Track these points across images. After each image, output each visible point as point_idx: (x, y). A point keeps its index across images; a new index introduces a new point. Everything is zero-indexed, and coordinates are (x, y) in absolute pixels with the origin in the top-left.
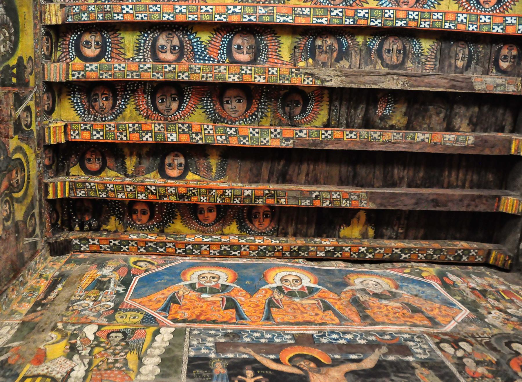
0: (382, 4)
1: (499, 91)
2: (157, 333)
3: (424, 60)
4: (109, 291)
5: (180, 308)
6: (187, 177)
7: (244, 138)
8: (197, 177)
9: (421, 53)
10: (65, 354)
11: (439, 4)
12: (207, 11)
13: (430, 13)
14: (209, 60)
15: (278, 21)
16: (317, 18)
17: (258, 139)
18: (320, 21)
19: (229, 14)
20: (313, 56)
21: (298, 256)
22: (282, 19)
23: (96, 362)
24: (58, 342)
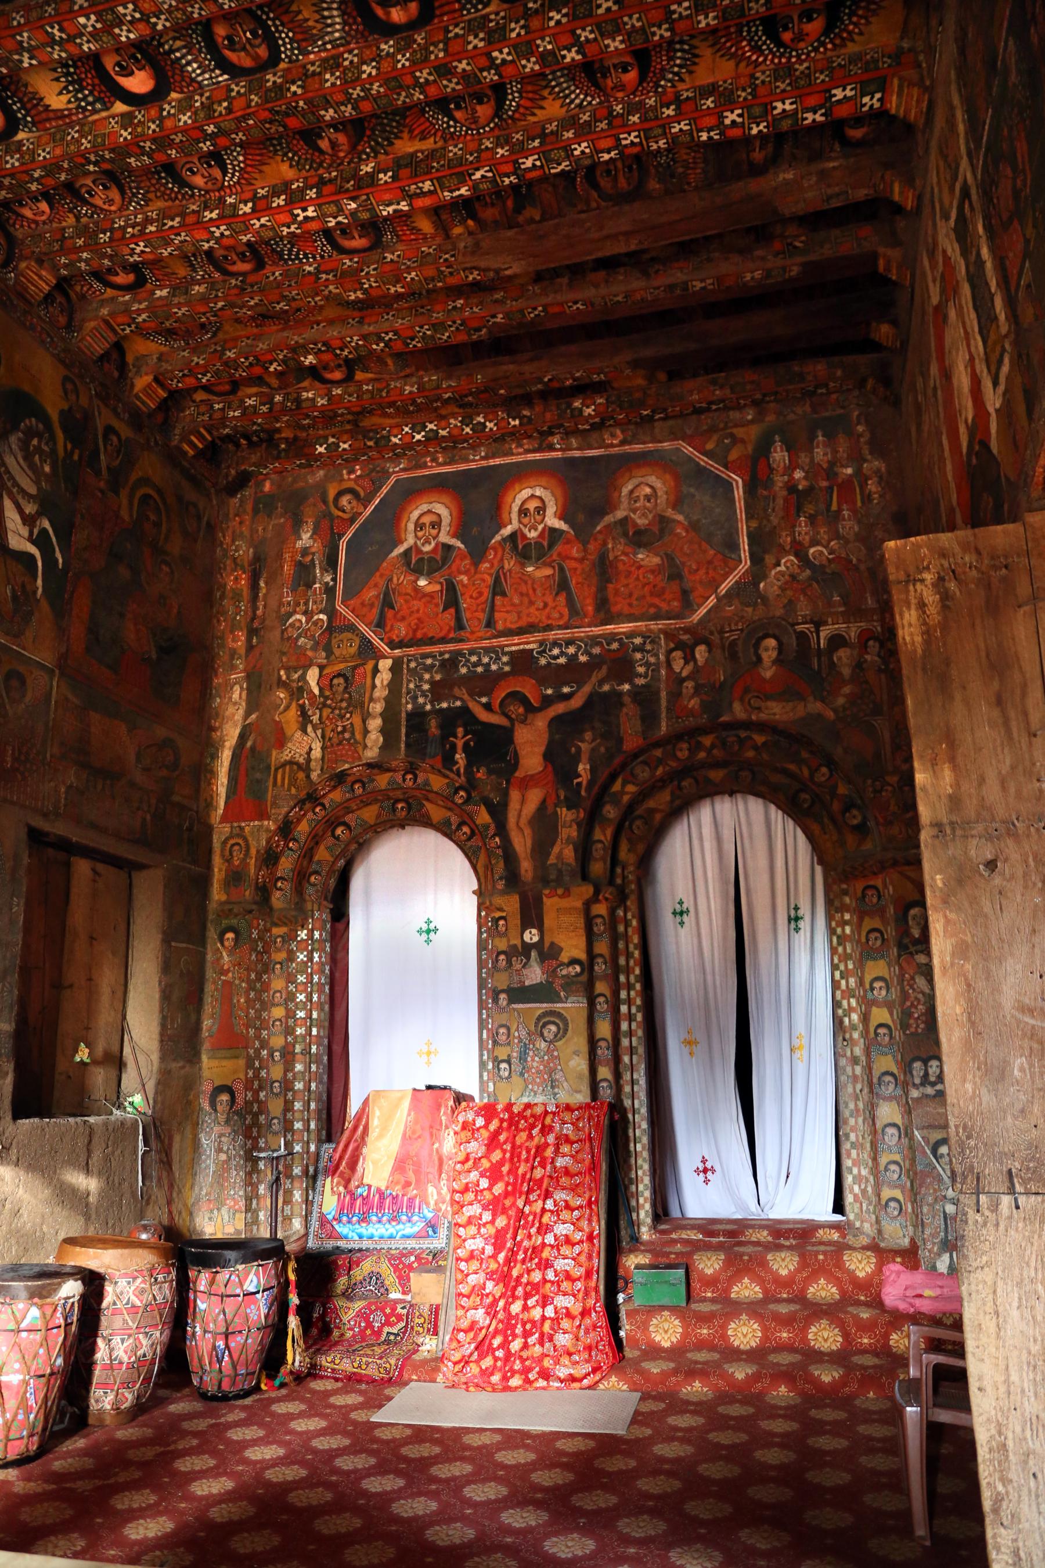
0: (572, 101)
1: (835, 203)
2: (376, 671)
3: (681, 170)
4: (317, 585)
7: (413, 339)
8: (370, 375)
9: (673, 159)
11: (690, 72)
12: (262, 226)
13: (663, 126)
15: (385, 213)
16: (451, 191)
17: (432, 337)
18: (457, 193)
19: (301, 223)
20: (473, 216)
21: (552, 434)
22: (391, 209)
23: (329, 734)
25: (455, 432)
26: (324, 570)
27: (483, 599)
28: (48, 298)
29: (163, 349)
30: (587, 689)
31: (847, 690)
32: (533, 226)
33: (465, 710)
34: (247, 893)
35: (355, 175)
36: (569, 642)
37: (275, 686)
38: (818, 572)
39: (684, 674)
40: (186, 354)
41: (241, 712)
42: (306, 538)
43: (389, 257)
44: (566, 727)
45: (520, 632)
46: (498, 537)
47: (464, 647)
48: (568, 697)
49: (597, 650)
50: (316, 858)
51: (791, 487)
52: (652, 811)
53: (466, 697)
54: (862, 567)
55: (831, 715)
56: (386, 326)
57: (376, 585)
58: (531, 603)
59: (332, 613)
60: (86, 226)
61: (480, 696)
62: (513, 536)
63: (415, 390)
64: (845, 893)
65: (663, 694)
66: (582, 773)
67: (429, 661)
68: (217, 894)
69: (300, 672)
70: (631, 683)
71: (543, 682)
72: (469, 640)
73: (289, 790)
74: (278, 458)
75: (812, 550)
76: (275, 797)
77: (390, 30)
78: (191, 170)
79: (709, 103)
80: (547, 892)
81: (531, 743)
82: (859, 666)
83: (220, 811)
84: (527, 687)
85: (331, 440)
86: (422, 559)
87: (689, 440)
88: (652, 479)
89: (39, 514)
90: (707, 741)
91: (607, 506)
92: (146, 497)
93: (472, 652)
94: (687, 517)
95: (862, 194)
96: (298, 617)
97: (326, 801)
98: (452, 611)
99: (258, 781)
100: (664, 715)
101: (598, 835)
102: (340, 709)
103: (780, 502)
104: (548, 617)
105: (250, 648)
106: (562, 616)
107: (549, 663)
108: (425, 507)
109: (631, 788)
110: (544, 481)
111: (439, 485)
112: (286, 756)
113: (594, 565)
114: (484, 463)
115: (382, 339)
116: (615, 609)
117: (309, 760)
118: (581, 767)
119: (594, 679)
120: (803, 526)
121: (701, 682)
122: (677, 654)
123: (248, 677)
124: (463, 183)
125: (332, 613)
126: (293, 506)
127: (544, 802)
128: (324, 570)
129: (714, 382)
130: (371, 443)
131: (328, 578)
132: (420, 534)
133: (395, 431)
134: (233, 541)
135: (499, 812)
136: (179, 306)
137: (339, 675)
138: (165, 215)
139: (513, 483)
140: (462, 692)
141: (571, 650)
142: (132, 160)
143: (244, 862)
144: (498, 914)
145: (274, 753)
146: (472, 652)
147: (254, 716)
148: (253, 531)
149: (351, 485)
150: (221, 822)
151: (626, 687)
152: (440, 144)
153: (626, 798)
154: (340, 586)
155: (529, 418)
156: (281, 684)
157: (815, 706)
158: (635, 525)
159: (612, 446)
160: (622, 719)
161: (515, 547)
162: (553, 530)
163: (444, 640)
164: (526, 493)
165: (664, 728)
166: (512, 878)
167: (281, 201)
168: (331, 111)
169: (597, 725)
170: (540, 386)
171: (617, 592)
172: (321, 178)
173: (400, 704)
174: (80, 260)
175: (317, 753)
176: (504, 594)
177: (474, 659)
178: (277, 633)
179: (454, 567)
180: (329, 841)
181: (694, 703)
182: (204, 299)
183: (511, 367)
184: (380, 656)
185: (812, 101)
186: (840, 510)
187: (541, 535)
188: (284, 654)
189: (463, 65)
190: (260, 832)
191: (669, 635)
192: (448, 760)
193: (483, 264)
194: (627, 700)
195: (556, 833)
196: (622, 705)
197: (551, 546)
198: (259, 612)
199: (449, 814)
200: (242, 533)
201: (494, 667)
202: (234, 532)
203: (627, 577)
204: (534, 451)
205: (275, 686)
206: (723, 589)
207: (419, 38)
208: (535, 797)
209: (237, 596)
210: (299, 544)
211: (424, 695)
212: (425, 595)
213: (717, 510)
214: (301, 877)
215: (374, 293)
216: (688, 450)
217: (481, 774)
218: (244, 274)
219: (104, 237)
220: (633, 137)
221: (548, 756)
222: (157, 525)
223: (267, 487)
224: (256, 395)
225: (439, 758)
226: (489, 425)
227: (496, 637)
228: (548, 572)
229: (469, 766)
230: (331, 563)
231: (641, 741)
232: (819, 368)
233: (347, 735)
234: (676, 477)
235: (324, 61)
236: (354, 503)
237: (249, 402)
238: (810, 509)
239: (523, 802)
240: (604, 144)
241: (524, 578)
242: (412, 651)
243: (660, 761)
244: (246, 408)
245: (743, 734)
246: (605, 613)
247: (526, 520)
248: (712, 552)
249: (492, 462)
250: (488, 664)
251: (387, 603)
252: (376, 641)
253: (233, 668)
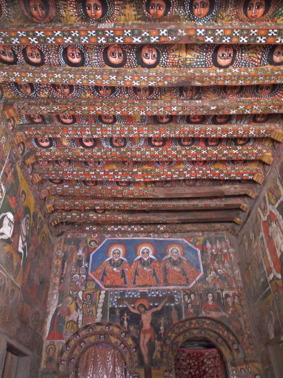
2: (100, 294)
4: (83, 267)
5: (106, 278)
6: (106, 213)
10: (75, 309)
14: (109, 185)
21: (151, 233)
24: (72, 303)
25: (126, 229)
26: (85, 262)
28: (36, 184)
29: (57, 198)
30: (162, 304)
31: (231, 309)
32: (168, 188)
33: (127, 308)
34: (54, 366)
35: (132, 171)
36: (157, 290)
37: (68, 296)
38: (221, 276)
39: (189, 302)
40: (63, 200)
41: (56, 303)
42: (80, 252)
43: (131, 189)
44: (157, 315)
45: (143, 286)
46: (136, 259)
47: (127, 289)
48: (157, 306)
49: (164, 293)
50: (74, 353)
51: (212, 254)
52: (178, 342)
53: (127, 304)
54: (231, 276)
55: (228, 317)
56: (121, 203)
57: (101, 268)
58: (146, 278)
59: (87, 275)
60: (56, 169)
61: (132, 304)
62: (140, 259)
63: (121, 218)
64: (234, 370)
65: (183, 307)
67: (116, 292)
68: (43, 366)
69: (76, 292)
70: (174, 303)
71: (150, 301)
73: (71, 330)
74: (74, 229)
75: (218, 271)
76: (66, 332)
77: (154, 146)
78: (91, 163)
79: (218, 172)
80: (152, 368)
81: (146, 319)
82: (233, 303)
83: (47, 336)
84: (145, 302)
85: (91, 226)
86: (115, 263)
87: (186, 239)
88: (177, 248)
89: (25, 241)
90: (194, 321)
91: (166, 254)
92: (43, 237)
93: (129, 291)
94: (186, 259)
95: (242, 193)
96: (77, 275)
97: (80, 334)
99: (60, 326)
100: (184, 314)
101: (165, 349)
102: (89, 305)
103: (210, 257)
104: (151, 283)
105: (60, 283)
106: (154, 283)
107: (151, 296)
108: (115, 248)
109: (173, 335)
110: (149, 245)
111: (120, 242)
112: (70, 318)
113: (163, 269)
114: (132, 238)
115: (119, 206)
116: (169, 282)
117: (78, 320)
118: (161, 328)
119: (164, 302)
120: (216, 264)
121: (194, 304)
122: (186, 296)
123: (60, 292)
124: (158, 178)
125: (87, 275)
126: (77, 243)
127: (151, 338)
128: (85, 262)
129: (193, 225)
130: (102, 229)
131: (86, 265)
132: (114, 255)
133: (109, 227)
134: (57, 251)
135: (136, 340)
136: (71, 190)
137: (89, 294)
138: (79, 170)
139: (140, 244)
140: (126, 303)
141: (157, 293)
142: (80, 159)
143: (54, 354)
144: (135, 375)
145: (67, 317)
146: (129, 291)
147: (60, 305)
148: (64, 248)
149: (95, 239)
150: (46, 340)
151: (173, 305)
152: (154, 168)
153: (172, 338)
154: (90, 268)
155: (146, 228)
156: (70, 295)
157: (223, 314)
158: (173, 259)
159: (166, 238)
160: (172, 314)
161: (141, 262)
162: (151, 259)
163: (121, 287)
164: (144, 248)
165: (184, 318)
166: (141, 363)
167: (112, 173)
168: (135, 159)
169: (165, 315)
170: (153, 222)
171: (169, 278)
172: (123, 170)
173: (107, 305)
174: (51, 176)
175: (81, 318)
176: (138, 275)
177: (130, 293)
178: (69, 280)
179: (124, 266)
180: (79, 347)
181: (192, 311)
182: (79, 190)
183: (147, 216)
184: (101, 289)
185: (239, 175)
186: (224, 261)
187: (148, 259)
188: (71, 286)
189: (170, 156)
190: (60, 344)
191: (184, 291)
192: (122, 323)
193: (155, 195)
194: (173, 308)
195: (155, 349)
196: (172, 310)
197: (151, 262)
198: (64, 272)
199: (117, 340)
200: (60, 248)
201: (135, 296)
202: (58, 248)
203: (172, 273)
204: (146, 237)
205: (68, 296)
206: (197, 279)
207: (160, 149)
208: (148, 336)
209: (57, 267)
210: (78, 254)
211: (115, 302)
212: (116, 273)
213: (194, 258)
214: (69, 359)
215: (125, 196)
216: (186, 241)
217: (132, 328)
218: (91, 186)
219: (61, 172)
220: (200, 175)
221: (152, 324)
222: (44, 245)
223: (69, 236)
224: (76, 213)
226: (135, 229)
227: (136, 287)
228: (150, 270)
229: (128, 325)
230: (88, 260)
231: (178, 321)
232: (218, 225)
233: (91, 313)
234: (183, 248)
235: (136, 149)
236: (95, 244)
237: (74, 214)
238: (217, 260)
239: (145, 338)
240: (193, 175)
241: (143, 271)
242: (111, 289)
243: (181, 327)
244: (72, 216)
245: (203, 320)
246: (166, 282)
247: (144, 255)
248: (193, 269)
249: (134, 238)
250: (134, 295)
251: (104, 274)
252: (101, 285)
253: (55, 289)
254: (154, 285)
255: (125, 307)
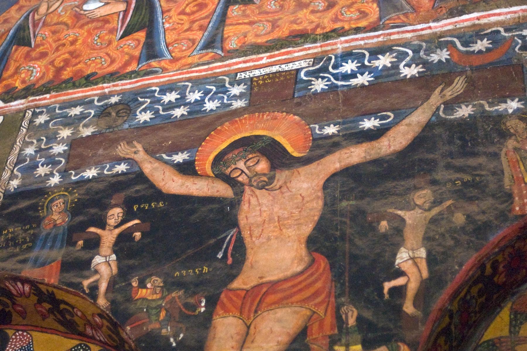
27: (205, 13)
47: (153, 82)
53: (141, 156)
61: (175, 149)
66: (407, 267)
67: (77, 111)
72: (164, 70)
98: (141, 35)
104: (336, 20)
107: (333, 88)
141: (384, 61)
196: (504, 135)
211: (52, 161)
212: (93, 21)
225: (56, 266)
242: (47, 99)
254: (363, 24)
255: (117, 175)
